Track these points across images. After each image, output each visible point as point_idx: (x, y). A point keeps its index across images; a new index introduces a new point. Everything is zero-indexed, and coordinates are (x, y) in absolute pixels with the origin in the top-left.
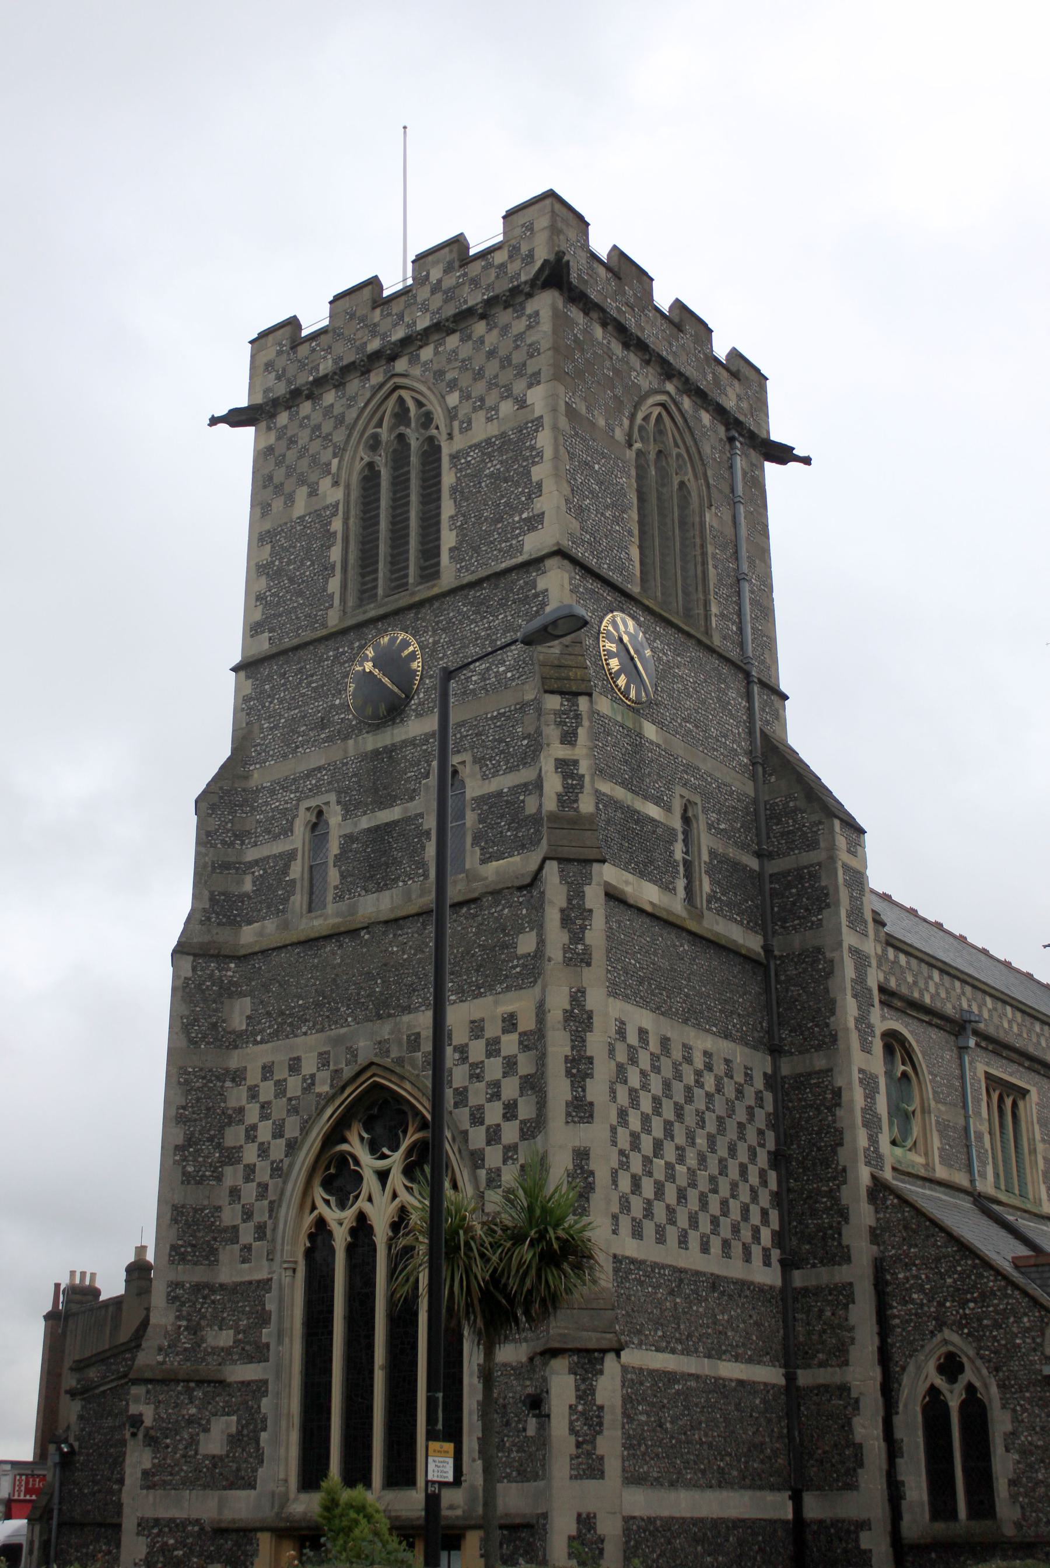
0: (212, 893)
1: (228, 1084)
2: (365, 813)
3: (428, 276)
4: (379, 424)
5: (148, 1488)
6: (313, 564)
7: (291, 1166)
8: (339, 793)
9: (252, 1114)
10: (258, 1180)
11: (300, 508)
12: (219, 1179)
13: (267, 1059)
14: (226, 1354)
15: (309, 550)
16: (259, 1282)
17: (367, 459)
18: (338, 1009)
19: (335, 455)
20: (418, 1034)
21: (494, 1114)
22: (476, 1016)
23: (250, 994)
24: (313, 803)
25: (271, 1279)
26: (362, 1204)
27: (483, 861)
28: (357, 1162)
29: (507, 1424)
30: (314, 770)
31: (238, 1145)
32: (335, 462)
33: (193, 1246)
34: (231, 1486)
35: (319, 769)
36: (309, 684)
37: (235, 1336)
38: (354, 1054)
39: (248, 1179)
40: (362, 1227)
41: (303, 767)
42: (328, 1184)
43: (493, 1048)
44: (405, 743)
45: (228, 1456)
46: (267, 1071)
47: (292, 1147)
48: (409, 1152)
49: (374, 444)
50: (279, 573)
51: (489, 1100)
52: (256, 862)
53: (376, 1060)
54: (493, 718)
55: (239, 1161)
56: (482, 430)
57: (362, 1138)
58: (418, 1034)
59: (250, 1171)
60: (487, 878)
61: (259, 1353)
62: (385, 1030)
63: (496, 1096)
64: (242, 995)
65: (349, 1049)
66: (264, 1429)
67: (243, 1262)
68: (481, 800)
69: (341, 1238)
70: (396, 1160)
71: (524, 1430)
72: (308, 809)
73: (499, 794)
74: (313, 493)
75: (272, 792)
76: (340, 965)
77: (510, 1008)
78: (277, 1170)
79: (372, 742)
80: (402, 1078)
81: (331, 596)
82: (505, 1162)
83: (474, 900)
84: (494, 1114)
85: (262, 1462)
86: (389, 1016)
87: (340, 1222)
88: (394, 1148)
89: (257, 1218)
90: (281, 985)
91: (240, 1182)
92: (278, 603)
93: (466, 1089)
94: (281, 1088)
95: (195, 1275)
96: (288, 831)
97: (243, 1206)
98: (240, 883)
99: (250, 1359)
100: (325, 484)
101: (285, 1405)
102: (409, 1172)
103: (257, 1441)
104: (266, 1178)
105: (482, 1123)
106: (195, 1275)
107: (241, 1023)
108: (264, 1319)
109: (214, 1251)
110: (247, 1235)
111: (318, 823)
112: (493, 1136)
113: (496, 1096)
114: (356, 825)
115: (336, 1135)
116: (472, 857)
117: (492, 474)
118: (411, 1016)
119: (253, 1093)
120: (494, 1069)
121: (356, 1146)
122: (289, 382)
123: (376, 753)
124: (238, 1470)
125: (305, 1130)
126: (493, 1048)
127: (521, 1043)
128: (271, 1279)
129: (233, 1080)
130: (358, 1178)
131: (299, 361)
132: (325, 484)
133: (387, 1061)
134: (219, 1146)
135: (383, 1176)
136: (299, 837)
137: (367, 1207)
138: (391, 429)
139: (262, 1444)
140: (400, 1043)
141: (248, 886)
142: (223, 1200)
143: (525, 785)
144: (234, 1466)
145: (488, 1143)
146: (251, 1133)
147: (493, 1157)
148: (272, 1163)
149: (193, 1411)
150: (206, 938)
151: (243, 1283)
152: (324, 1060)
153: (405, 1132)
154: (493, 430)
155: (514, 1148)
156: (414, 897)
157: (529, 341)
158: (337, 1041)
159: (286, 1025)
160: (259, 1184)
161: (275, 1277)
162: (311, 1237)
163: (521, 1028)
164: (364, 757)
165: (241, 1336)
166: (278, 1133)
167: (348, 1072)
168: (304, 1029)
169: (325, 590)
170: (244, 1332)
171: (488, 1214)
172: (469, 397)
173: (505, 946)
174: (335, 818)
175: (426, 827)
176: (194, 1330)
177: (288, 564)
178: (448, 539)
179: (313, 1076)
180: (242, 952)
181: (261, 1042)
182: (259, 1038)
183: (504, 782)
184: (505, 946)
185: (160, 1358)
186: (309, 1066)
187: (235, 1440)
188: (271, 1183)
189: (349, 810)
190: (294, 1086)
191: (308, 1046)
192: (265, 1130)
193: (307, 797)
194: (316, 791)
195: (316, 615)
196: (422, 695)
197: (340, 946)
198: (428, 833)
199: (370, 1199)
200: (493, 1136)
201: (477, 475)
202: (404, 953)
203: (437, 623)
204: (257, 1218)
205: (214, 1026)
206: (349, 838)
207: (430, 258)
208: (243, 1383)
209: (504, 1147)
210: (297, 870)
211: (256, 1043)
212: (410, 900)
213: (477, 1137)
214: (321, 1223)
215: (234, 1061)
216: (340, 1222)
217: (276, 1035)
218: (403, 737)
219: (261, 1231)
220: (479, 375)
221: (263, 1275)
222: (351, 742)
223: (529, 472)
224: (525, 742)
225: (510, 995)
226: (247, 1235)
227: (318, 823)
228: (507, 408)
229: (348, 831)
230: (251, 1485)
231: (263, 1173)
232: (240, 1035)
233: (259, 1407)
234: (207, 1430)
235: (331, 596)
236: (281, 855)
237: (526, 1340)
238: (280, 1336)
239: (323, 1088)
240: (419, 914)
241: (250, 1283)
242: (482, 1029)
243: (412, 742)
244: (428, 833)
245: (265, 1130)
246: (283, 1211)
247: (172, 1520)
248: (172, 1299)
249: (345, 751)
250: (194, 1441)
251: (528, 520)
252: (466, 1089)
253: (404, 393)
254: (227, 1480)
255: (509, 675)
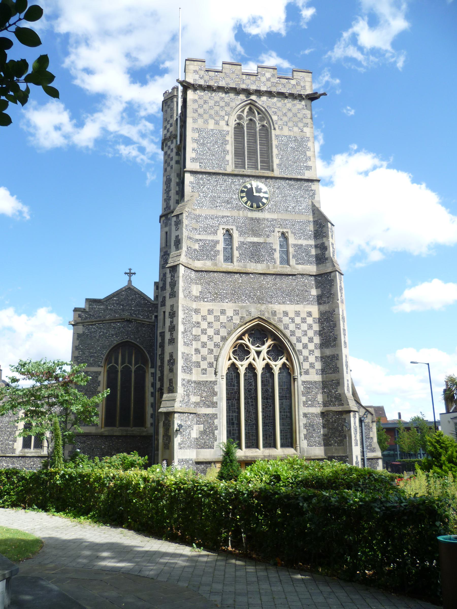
0: (187, 246)
1: (193, 313)
2: (249, 237)
3: (265, 74)
4: (243, 112)
5: (181, 448)
6: (218, 147)
7: (224, 344)
8: (237, 227)
9: (204, 325)
10: (208, 347)
11: (211, 125)
12: (192, 345)
13: (211, 308)
14: (197, 404)
15: (216, 142)
16: (211, 382)
17: (238, 121)
18: (241, 297)
19: (226, 115)
20: (275, 311)
21: (305, 340)
22: (297, 310)
23: (201, 284)
24: (226, 227)
25: (217, 381)
26: (250, 360)
27: (297, 264)
28: (247, 346)
29: (314, 430)
30: (226, 216)
31: (198, 334)
32: (226, 118)
33: (187, 367)
34: (203, 448)
35: (228, 216)
36: (221, 187)
37: (200, 398)
38: (250, 313)
39: (203, 347)
40: (251, 368)
41: (221, 214)
42: (234, 352)
43: (304, 320)
44: (264, 219)
45: (199, 438)
46: (210, 312)
47: (224, 339)
48: (269, 347)
49: (240, 117)
50: (203, 144)
51: (304, 336)
52: (200, 240)
53: (260, 316)
54: (298, 222)
55: (199, 340)
56: (286, 132)
57: (249, 340)
58: (275, 311)
59: (204, 345)
60: (298, 269)
61: (214, 405)
62: (263, 307)
63: (306, 335)
64: (196, 284)
65: (247, 311)
66: (217, 430)
67: (203, 374)
68: (295, 245)
69: (242, 371)
70: (264, 349)
71: (320, 432)
72: (223, 229)
73: (302, 245)
74: (217, 123)
75: (206, 218)
76: (241, 283)
77: (310, 310)
78: (216, 345)
79: (251, 215)
80: (270, 324)
81: (228, 161)
82: (310, 354)
83: (295, 275)
84: (305, 340)
85: (216, 440)
86: (263, 303)
87: (242, 366)
88: (263, 344)
89: (208, 360)
90: (215, 284)
91: (199, 347)
92: (203, 155)
93: (294, 331)
94: (217, 319)
95: (187, 377)
96: (215, 233)
97: (202, 356)
98: (194, 245)
99: (209, 407)
100: (222, 123)
101: (222, 423)
102: (268, 353)
103: (214, 434)
104: (212, 347)
105: (301, 342)
106: (187, 377)
107: (197, 293)
108: (215, 394)
109: (191, 369)
110: (204, 365)
111: (229, 234)
112: (305, 346)
113: (306, 335)
114: (245, 239)
115: (240, 338)
116: (292, 262)
117: (292, 147)
118: (272, 305)
119: (204, 318)
120: (304, 327)
121: (246, 340)
122: (205, 81)
123: (252, 219)
124: (205, 442)
125: (230, 334)
126: (304, 320)
127: (313, 321)
128: (217, 381)
129: (195, 312)
130: (249, 353)
131: (210, 76)
132: (222, 123)
133: (264, 318)
134: (192, 334)
135: (258, 353)
136: (220, 236)
137: (253, 362)
138: (247, 116)
139: (216, 434)
140: (268, 312)
141: (197, 247)
142: (193, 352)
143: (311, 245)
144: (203, 442)
145: (304, 348)
146: (204, 332)
147: (305, 353)
148: (215, 343)
149: (189, 423)
150: (186, 261)
151: (204, 381)
152: (236, 313)
153: (267, 341)
154: (291, 134)
155: (313, 351)
156: (270, 268)
157: (303, 113)
158: (242, 307)
159: (217, 297)
160: (209, 349)
161: (218, 380)
162: (228, 369)
163: (313, 316)
164: (247, 218)
165: (203, 399)
166: (217, 333)
167: (248, 319)
168: (227, 301)
169: (224, 158)
170: (205, 397)
171: (304, 369)
172: (281, 120)
173: (306, 291)
174: (236, 235)
175: (274, 247)
176: (188, 395)
177: (207, 143)
178: (276, 161)
179: (231, 317)
180: (196, 269)
181: (207, 301)
182: (206, 300)
183: (300, 242)
184: (306, 291)
185: (181, 405)
186: (230, 313)
187: (203, 433)
188: (214, 349)
189: (241, 233)
190: (223, 319)
191: (230, 307)
192: (210, 332)
193: (223, 225)
194: (227, 223)
195: (221, 165)
196: (270, 206)
197: (241, 277)
198: (275, 250)
199: (254, 359)
200: (305, 346)
201: (286, 145)
202: (268, 285)
203: (275, 185)
204: (208, 360)
205: (190, 292)
206: (243, 243)
207: (265, 69)
208: (205, 414)
209: (309, 350)
210: (220, 247)
211: (204, 301)
212: (269, 268)
213: (299, 346)
214: (233, 365)
215: (194, 305)
216: (242, 366)
217: (214, 300)
218: (263, 217)
219: (211, 365)
220: (285, 115)
221: (213, 378)
222: (241, 212)
223: (305, 152)
224: (310, 233)
225: (310, 306)
226: (204, 365)
227: (229, 234)
228: (296, 129)
229: (242, 240)
230: (211, 447)
231: (210, 345)
232: (196, 297)
233: (213, 422)
234: (193, 429)
235: (228, 161)
236: (212, 241)
237: (319, 407)
238: (221, 399)
239: (236, 320)
240: (273, 274)
241: (207, 381)
242: (299, 314)
243: (267, 220)
244: (275, 250)
245: (210, 332)
246: (220, 360)
247: (186, 459)
248: (183, 385)
249: (239, 214)
250: (190, 434)
251: (306, 166)
252: (294, 331)
253: (252, 107)
254: (200, 446)
255: (303, 211)
